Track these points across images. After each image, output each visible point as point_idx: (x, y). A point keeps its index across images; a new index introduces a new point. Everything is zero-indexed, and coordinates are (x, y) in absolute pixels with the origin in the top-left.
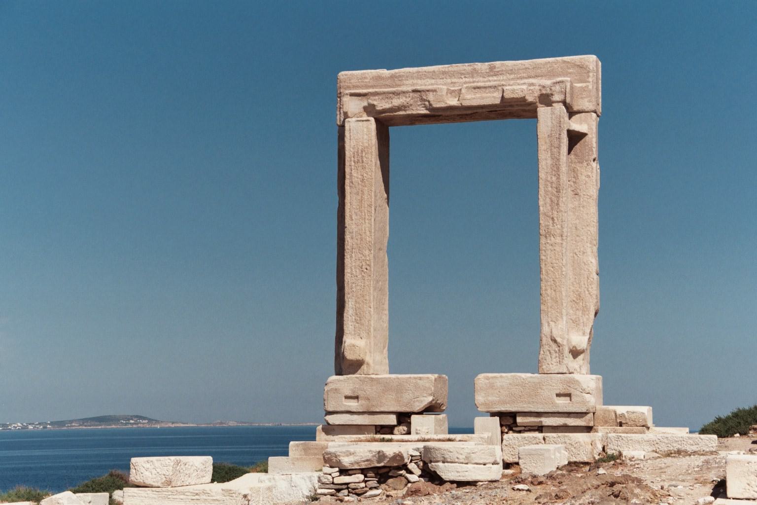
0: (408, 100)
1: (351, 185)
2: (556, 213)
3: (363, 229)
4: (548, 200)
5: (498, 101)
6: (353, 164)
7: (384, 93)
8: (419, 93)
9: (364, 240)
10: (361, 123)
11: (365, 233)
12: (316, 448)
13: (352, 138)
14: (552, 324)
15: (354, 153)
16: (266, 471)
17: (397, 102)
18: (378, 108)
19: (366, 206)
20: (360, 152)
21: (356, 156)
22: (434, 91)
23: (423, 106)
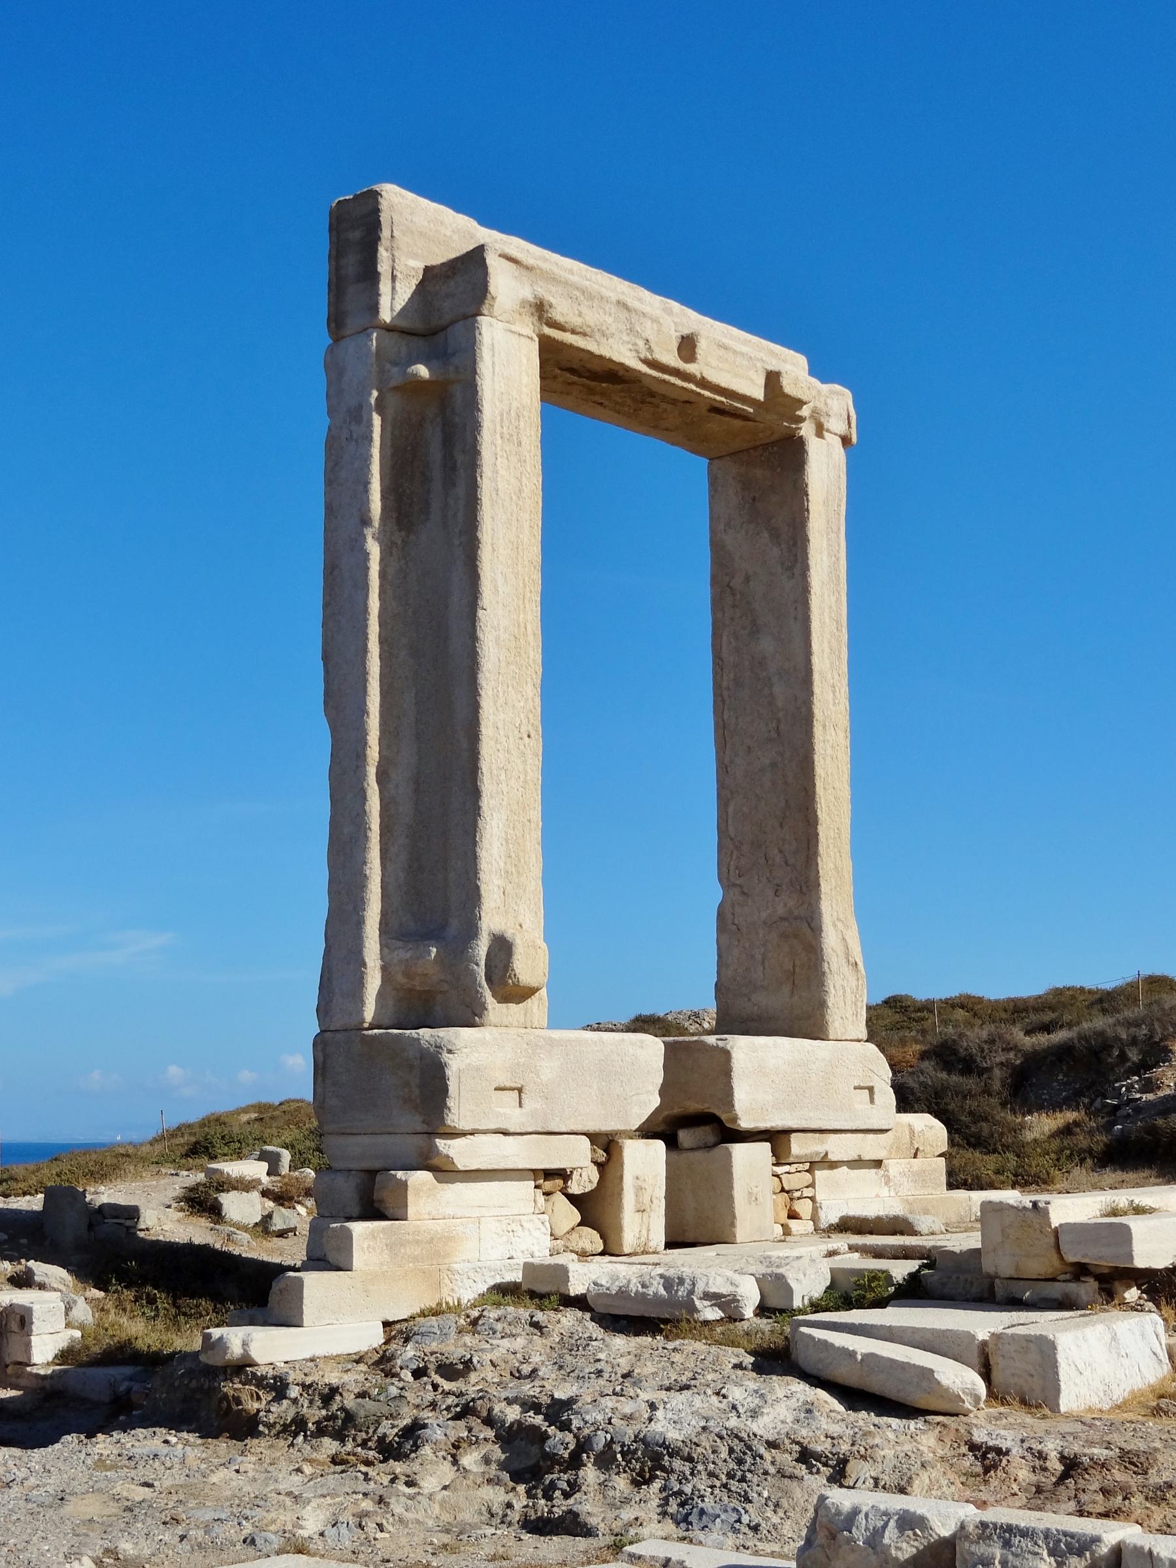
0: (610, 320)
1: (494, 496)
2: (836, 677)
3: (522, 625)
4: (826, 645)
5: (759, 394)
6: (499, 442)
7: (566, 283)
8: (626, 314)
9: (523, 653)
10: (514, 339)
11: (526, 635)
12: (417, 1242)
13: (497, 369)
14: (840, 925)
15: (502, 415)
16: (299, 1325)
17: (591, 317)
18: (559, 318)
19: (526, 563)
20: (513, 414)
21: (506, 423)
22: (655, 320)
23: (630, 346)
